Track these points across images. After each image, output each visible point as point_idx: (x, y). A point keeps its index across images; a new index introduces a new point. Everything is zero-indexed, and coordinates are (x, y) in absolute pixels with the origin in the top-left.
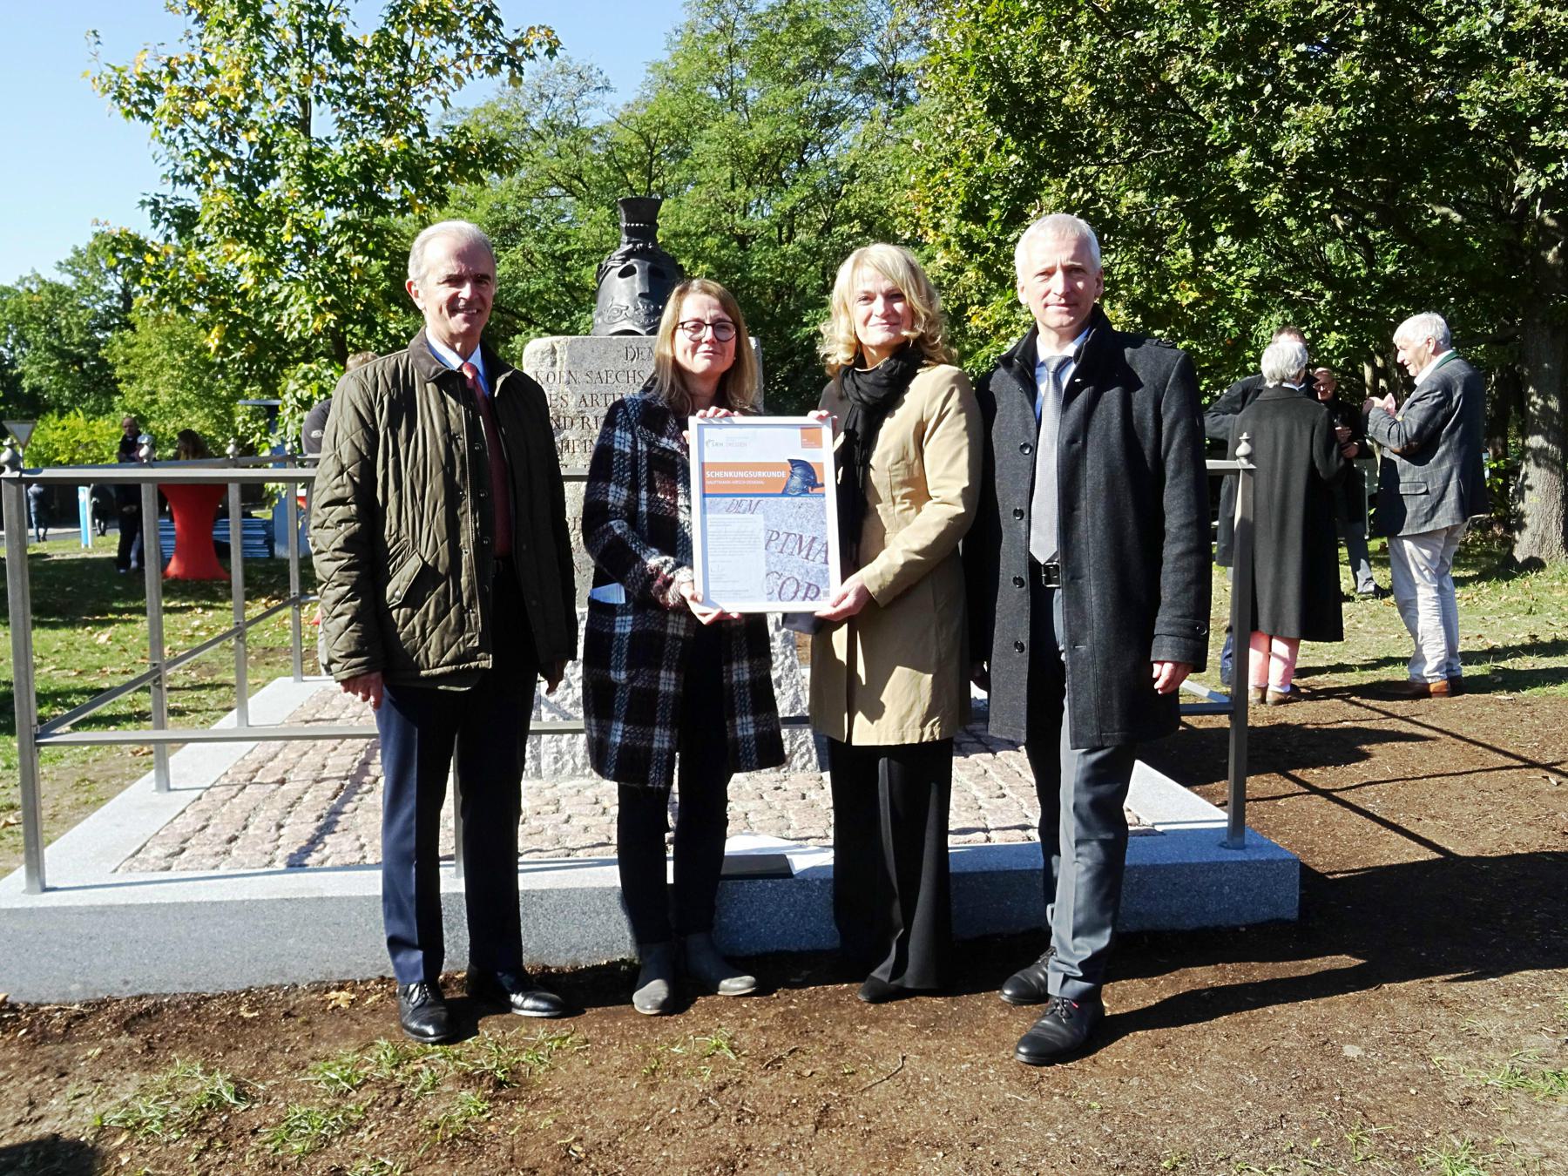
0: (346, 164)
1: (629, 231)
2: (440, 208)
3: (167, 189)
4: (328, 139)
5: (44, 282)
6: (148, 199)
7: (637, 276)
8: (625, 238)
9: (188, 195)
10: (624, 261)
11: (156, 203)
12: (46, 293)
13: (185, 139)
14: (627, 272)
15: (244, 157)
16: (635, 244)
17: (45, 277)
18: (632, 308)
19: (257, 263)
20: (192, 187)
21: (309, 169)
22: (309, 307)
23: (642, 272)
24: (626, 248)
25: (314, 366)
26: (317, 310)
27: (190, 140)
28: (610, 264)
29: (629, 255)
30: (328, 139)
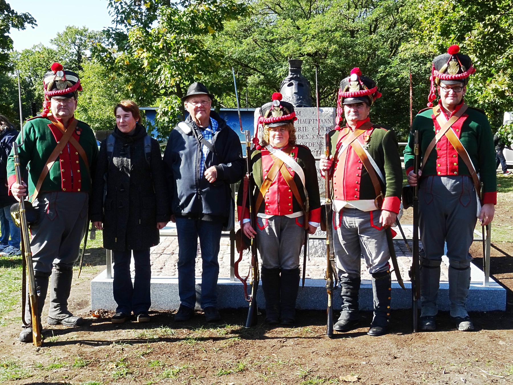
0: (185, 17)
1: (291, 71)
2: (219, 31)
3: (114, 26)
4: (176, 3)
5: (45, 49)
6: (106, 29)
7: (294, 86)
8: (290, 73)
9: (122, 28)
10: (290, 81)
11: (109, 31)
12: (46, 53)
13: (122, 6)
14: (290, 85)
15: (143, 11)
16: (293, 75)
17: (45, 46)
18: (291, 98)
19: (149, 57)
20: (123, 25)
21: (170, 19)
22: (169, 75)
23: (296, 85)
24: (290, 76)
25: (170, 99)
26: (172, 76)
27: (124, 6)
28: (285, 82)
29: (291, 79)
30: (176, 3)
